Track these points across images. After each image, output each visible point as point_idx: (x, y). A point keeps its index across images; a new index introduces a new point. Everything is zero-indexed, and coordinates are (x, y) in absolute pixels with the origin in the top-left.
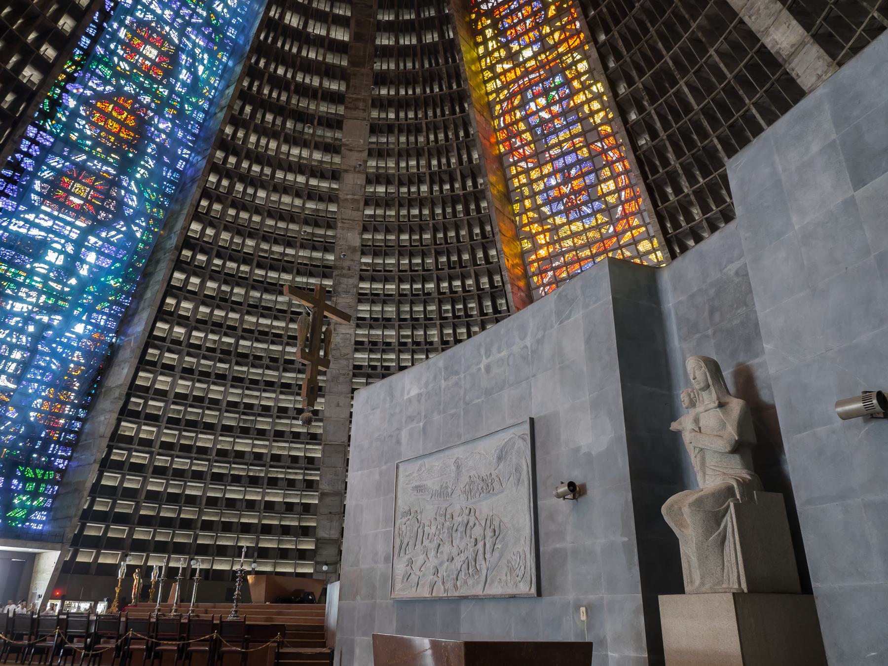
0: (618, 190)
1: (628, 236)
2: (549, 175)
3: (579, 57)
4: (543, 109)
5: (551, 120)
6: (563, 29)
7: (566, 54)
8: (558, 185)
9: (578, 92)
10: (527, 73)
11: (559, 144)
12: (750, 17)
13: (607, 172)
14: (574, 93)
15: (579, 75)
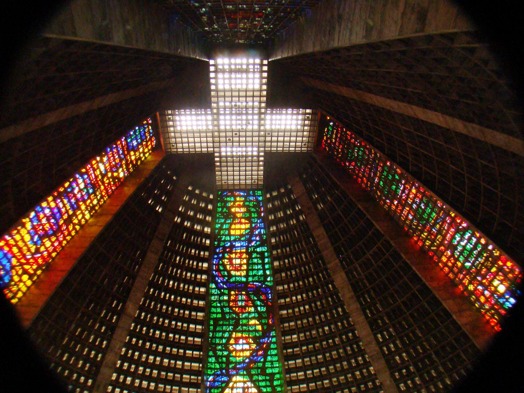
0: (47, 249)
1: (27, 267)
2: (50, 208)
5: (75, 195)
6: (109, 183)
8: (45, 215)
9: (85, 204)
10: (94, 170)
11: (64, 206)
12: (134, 292)
13: (54, 239)
14: (84, 201)
15: (91, 202)
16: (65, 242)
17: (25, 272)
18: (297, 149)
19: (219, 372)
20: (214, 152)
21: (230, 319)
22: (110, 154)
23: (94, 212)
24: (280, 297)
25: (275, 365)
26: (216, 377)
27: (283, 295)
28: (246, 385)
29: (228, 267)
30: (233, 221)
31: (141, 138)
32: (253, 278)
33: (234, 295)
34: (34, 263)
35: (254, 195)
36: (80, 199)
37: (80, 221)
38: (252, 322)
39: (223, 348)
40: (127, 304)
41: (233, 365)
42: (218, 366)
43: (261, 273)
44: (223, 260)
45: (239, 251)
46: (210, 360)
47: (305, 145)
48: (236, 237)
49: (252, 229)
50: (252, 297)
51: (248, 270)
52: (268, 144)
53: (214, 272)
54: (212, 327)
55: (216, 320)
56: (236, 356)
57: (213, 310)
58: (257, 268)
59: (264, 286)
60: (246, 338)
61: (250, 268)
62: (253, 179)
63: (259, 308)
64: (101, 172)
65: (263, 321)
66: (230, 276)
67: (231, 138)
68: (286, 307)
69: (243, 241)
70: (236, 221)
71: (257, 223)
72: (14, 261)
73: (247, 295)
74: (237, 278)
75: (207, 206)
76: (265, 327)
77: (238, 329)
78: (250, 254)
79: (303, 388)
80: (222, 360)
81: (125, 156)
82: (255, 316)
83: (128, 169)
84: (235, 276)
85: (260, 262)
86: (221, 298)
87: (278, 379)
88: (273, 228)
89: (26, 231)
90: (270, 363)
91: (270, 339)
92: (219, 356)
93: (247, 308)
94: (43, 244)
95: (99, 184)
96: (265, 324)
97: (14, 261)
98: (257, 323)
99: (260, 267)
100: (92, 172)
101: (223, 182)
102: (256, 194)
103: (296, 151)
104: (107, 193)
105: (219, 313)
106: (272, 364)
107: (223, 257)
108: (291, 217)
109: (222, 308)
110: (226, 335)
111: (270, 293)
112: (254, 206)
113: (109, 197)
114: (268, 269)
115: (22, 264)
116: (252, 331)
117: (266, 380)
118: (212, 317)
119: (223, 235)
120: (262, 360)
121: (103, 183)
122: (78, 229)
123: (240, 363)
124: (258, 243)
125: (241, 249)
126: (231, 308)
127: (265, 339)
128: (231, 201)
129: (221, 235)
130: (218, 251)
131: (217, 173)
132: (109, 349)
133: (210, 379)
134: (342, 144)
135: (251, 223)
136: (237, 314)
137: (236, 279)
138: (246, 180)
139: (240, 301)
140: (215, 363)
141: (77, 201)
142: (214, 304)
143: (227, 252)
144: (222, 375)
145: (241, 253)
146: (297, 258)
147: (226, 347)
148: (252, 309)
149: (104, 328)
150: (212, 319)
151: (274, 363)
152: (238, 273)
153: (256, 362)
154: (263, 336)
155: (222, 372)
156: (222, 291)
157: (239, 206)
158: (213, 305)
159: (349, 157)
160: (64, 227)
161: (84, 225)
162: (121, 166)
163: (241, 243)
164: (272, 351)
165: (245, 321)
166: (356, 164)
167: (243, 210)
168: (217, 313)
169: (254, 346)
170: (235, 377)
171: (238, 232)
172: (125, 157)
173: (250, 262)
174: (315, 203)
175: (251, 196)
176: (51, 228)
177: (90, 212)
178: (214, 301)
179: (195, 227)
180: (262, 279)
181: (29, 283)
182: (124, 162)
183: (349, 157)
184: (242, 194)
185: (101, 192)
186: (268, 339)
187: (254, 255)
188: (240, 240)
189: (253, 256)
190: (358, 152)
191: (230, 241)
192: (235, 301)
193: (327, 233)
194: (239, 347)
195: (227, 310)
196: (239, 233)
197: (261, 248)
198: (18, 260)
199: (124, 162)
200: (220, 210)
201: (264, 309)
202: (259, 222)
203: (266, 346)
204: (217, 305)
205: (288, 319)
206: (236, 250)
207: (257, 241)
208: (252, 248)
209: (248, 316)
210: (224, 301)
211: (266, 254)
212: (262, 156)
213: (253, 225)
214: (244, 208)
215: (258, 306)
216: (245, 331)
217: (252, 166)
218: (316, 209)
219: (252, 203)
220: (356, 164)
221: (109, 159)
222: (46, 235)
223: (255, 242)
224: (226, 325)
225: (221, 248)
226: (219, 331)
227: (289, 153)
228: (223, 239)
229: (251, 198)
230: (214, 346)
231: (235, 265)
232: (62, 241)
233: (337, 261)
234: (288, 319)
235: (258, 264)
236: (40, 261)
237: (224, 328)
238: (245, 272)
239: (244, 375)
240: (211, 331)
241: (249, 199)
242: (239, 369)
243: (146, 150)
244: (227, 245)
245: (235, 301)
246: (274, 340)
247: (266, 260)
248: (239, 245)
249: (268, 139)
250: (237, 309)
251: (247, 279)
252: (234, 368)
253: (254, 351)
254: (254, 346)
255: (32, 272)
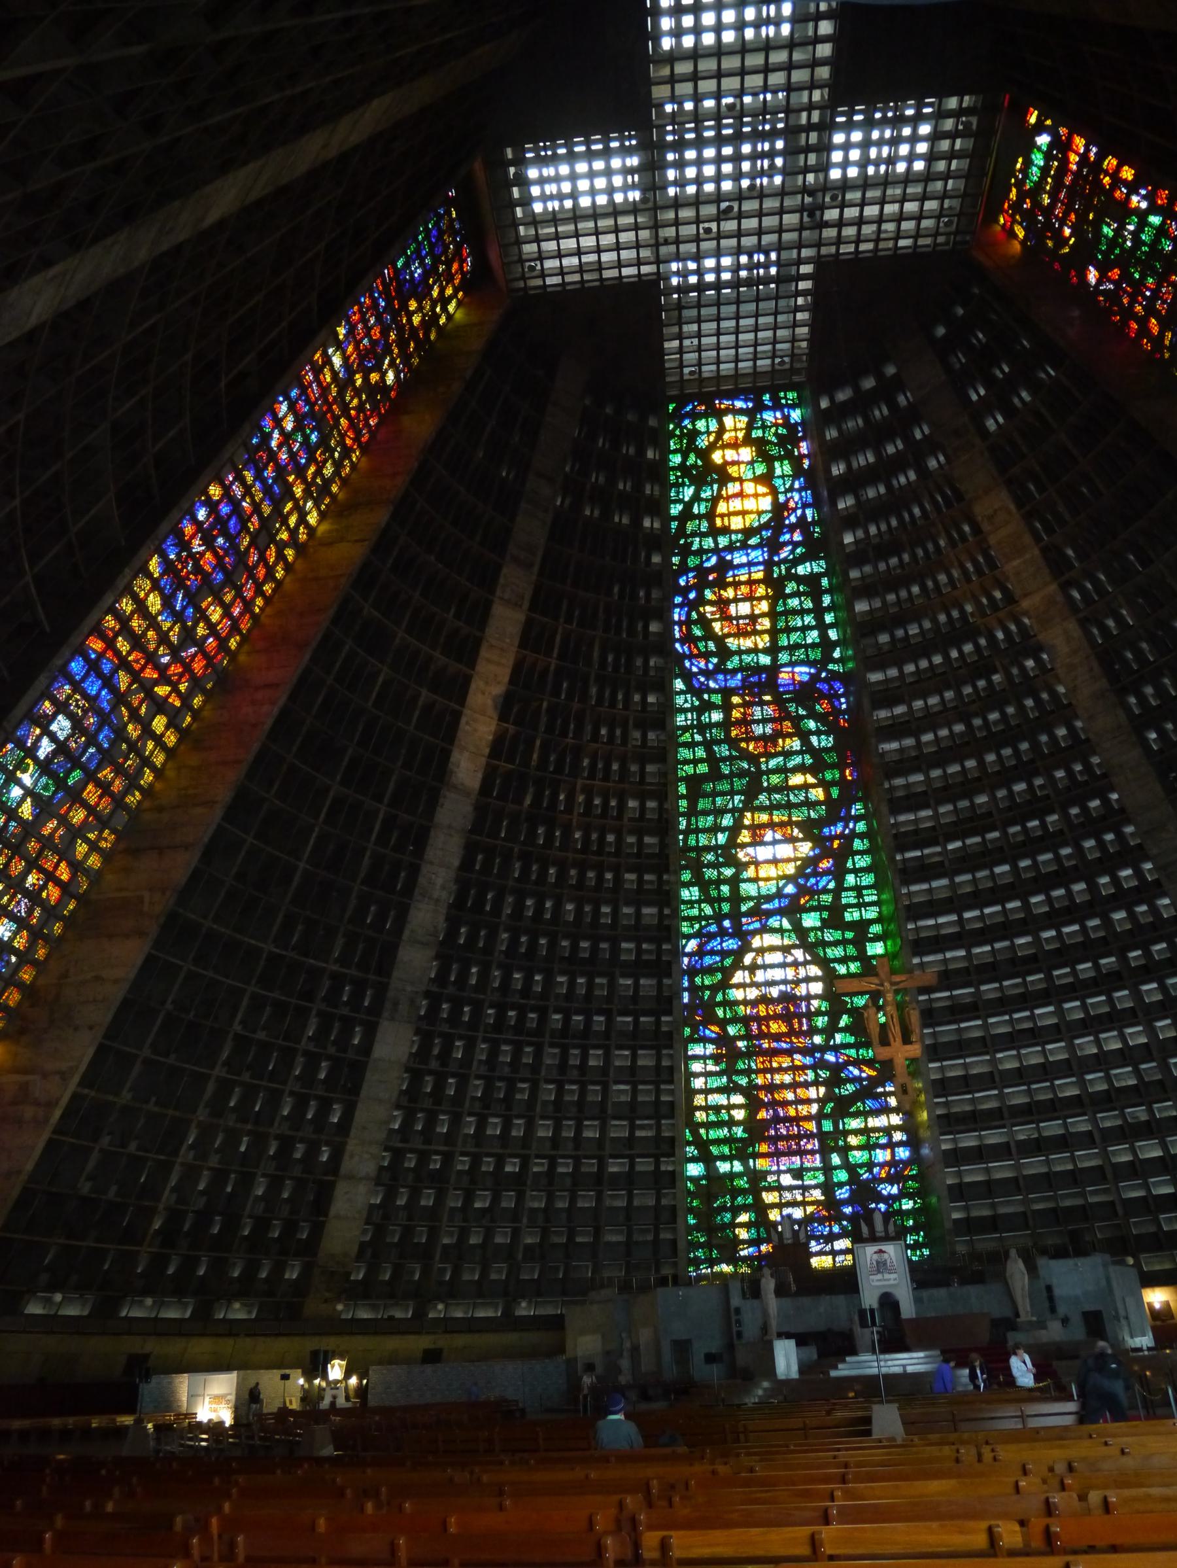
0: (211, 627)
1: (162, 690)
3: (336, 455)
4: (282, 431)
5: (273, 456)
6: (360, 408)
7: (339, 431)
9: (304, 480)
10: (317, 371)
12: (467, 723)
14: (301, 472)
15: (319, 472)
16: (259, 602)
17: (160, 706)
18: (921, 242)
19: (713, 928)
20: (662, 277)
21: (732, 775)
22: (355, 314)
23: (327, 501)
24: (878, 704)
25: (867, 899)
26: (707, 943)
27: (887, 696)
28: (790, 959)
29: (717, 626)
30: (720, 489)
31: (431, 253)
32: (791, 655)
33: (739, 705)
34: (181, 675)
35: (777, 406)
36: (287, 464)
37: (293, 533)
38: (797, 779)
39: (721, 860)
40: (452, 759)
41: (751, 904)
42: (708, 910)
43: (813, 636)
44: (701, 609)
45: (744, 578)
46: (685, 894)
47: (946, 224)
48: (734, 537)
49: (779, 509)
50: (792, 707)
51: (774, 633)
52: (830, 233)
53: (677, 646)
54: (683, 803)
55: (694, 782)
56: (755, 880)
57: (684, 753)
58: (800, 624)
59: (824, 675)
60: (782, 825)
61: (781, 624)
62: (778, 353)
63: (814, 740)
64: (335, 374)
65: (828, 776)
66: (724, 653)
67: (714, 226)
68: (894, 730)
69: (754, 548)
70: (730, 493)
71: (791, 489)
72: (123, 680)
73: (779, 702)
74: (744, 657)
75: (641, 452)
76: (835, 793)
77: (757, 803)
78: (776, 586)
79: (954, 959)
80: (719, 891)
81: (396, 315)
82: (803, 763)
83: (406, 357)
84: (740, 652)
85: (809, 604)
86: (705, 718)
87: (877, 938)
88: (845, 503)
89: (148, 584)
90: (850, 893)
91: (851, 825)
92: (711, 882)
93: (780, 741)
94: (204, 616)
95: (332, 412)
96: (833, 783)
97: (123, 680)
98: (811, 780)
99: (809, 619)
100: (310, 377)
101: (686, 370)
102: (783, 401)
103: (919, 250)
104: (356, 440)
105: (701, 761)
106: (860, 895)
107: (701, 601)
108: (897, 464)
109: (708, 745)
110: (727, 821)
111: (842, 695)
112: (782, 441)
113: (364, 449)
114: (831, 626)
115: (147, 689)
116: (797, 806)
117: (843, 942)
118: (681, 774)
119: (694, 534)
120: (832, 885)
121: (345, 409)
122: (290, 559)
123: (769, 898)
124: (798, 551)
125: (750, 573)
126: (733, 743)
127: (835, 825)
128: (708, 433)
129: (686, 536)
130: (682, 582)
131: (667, 345)
132: (417, 891)
133: (688, 949)
134: (1076, 211)
135: (774, 492)
136: (753, 759)
137: (741, 660)
138: (755, 359)
139: (758, 722)
140: (699, 902)
141: (281, 471)
142: (687, 737)
143: (711, 585)
144: (722, 933)
145: (751, 583)
146: (923, 587)
147: (727, 854)
148: (796, 744)
149: (395, 835)
150: (682, 779)
151: (865, 892)
152: (747, 643)
153: (813, 892)
154: (831, 820)
155: (720, 926)
156: (706, 696)
157: (735, 445)
158: (682, 739)
159: (1102, 252)
160: (254, 557)
161: (305, 544)
162: (388, 351)
163: (748, 555)
164: (857, 858)
165: (775, 779)
166: (1126, 276)
167: (746, 453)
168: (695, 762)
169: (805, 849)
170: (758, 937)
171: (737, 523)
172: (394, 320)
173: (780, 609)
174: (978, 412)
175: (767, 408)
176: (220, 565)
177: (317, 505)
178: (685, 729)
179: (617, 519)
180: (815, 655)
181: (171, 739)
182: (393, 336)
183: (1102, 252)
184: (739, 404)
185: (343, 436)
186: (846, 826)
187: (791, 587)
188: (744, 546)
189: (788, 591)
190: (1136, 235)
191: (716, 551)
192: (745, 722)
193: (1020, 505)
194: (763, 853)
195: (723, 750)
196: (741, 526)
197: (808, 564)
198: (135, 676)
199: (393, 336)
200: (676, 459)
201: (827, 742)
202: (797, 485)
203: (839, 845)
204: (692, 736)
205: (903, 765)
206: (734, 576)
207: (796, 545)
208: (783, 567)
209: (785, 764)
210: (711, 725)
211: (825, 582)
212: (805, 277)
213: (782, 498)
214: (748, 449)
215: (811, 733)
216: (778, 807)
217: (776, 313)
218: (983, 432)
219: (773, 430)
220: (1126, 276)
221: (351, 332)
222: (208, 586)
223: (790, 547)
224: (722, 794)
225: (691, 575)
226: (705, 813)
227: (896, 255)
228: (695, 547)
229: (769, 416)
230: (693, 855)
231: (738, 618)
232: (253, 599)
233: (1053, 587)
234: (903, 765)
235: (802, 612)
236: (198, 666)
237: (719, 800)
238: (766, 638)
239: (781, 931)
240: (683, 814)
241: (762, 419)
242: (770, 914)
243: (449, 291)
244: (707, 565)
245: (745, 722)
246: (861, 827)
247: (827, 600)
248: (744, 560)
249: (832, 214)
250: (751, 747)
251: (775, 660)
252: (755, 912)
253: (812, 861)
254: (805, 849)
255: (178, 703)
